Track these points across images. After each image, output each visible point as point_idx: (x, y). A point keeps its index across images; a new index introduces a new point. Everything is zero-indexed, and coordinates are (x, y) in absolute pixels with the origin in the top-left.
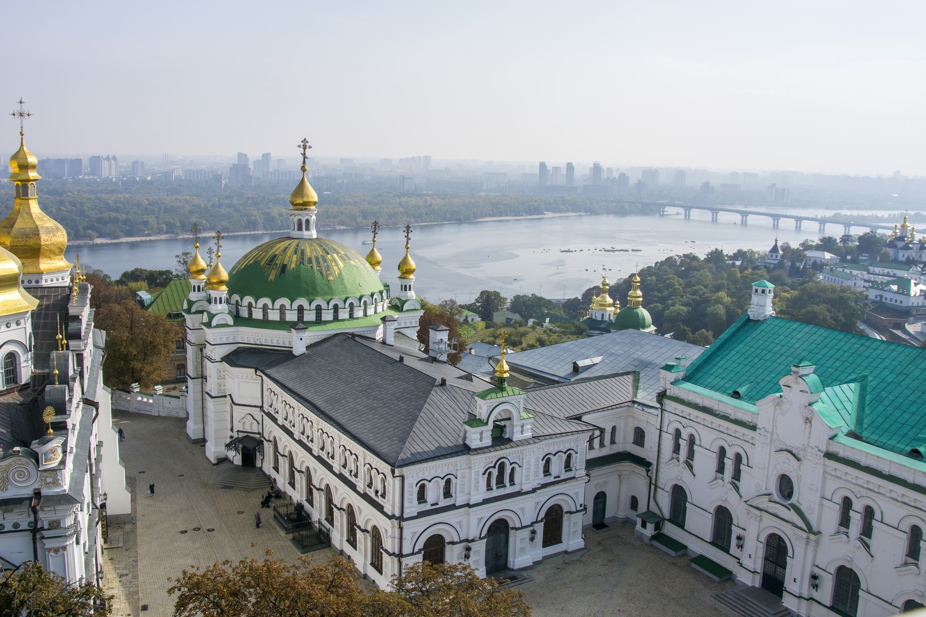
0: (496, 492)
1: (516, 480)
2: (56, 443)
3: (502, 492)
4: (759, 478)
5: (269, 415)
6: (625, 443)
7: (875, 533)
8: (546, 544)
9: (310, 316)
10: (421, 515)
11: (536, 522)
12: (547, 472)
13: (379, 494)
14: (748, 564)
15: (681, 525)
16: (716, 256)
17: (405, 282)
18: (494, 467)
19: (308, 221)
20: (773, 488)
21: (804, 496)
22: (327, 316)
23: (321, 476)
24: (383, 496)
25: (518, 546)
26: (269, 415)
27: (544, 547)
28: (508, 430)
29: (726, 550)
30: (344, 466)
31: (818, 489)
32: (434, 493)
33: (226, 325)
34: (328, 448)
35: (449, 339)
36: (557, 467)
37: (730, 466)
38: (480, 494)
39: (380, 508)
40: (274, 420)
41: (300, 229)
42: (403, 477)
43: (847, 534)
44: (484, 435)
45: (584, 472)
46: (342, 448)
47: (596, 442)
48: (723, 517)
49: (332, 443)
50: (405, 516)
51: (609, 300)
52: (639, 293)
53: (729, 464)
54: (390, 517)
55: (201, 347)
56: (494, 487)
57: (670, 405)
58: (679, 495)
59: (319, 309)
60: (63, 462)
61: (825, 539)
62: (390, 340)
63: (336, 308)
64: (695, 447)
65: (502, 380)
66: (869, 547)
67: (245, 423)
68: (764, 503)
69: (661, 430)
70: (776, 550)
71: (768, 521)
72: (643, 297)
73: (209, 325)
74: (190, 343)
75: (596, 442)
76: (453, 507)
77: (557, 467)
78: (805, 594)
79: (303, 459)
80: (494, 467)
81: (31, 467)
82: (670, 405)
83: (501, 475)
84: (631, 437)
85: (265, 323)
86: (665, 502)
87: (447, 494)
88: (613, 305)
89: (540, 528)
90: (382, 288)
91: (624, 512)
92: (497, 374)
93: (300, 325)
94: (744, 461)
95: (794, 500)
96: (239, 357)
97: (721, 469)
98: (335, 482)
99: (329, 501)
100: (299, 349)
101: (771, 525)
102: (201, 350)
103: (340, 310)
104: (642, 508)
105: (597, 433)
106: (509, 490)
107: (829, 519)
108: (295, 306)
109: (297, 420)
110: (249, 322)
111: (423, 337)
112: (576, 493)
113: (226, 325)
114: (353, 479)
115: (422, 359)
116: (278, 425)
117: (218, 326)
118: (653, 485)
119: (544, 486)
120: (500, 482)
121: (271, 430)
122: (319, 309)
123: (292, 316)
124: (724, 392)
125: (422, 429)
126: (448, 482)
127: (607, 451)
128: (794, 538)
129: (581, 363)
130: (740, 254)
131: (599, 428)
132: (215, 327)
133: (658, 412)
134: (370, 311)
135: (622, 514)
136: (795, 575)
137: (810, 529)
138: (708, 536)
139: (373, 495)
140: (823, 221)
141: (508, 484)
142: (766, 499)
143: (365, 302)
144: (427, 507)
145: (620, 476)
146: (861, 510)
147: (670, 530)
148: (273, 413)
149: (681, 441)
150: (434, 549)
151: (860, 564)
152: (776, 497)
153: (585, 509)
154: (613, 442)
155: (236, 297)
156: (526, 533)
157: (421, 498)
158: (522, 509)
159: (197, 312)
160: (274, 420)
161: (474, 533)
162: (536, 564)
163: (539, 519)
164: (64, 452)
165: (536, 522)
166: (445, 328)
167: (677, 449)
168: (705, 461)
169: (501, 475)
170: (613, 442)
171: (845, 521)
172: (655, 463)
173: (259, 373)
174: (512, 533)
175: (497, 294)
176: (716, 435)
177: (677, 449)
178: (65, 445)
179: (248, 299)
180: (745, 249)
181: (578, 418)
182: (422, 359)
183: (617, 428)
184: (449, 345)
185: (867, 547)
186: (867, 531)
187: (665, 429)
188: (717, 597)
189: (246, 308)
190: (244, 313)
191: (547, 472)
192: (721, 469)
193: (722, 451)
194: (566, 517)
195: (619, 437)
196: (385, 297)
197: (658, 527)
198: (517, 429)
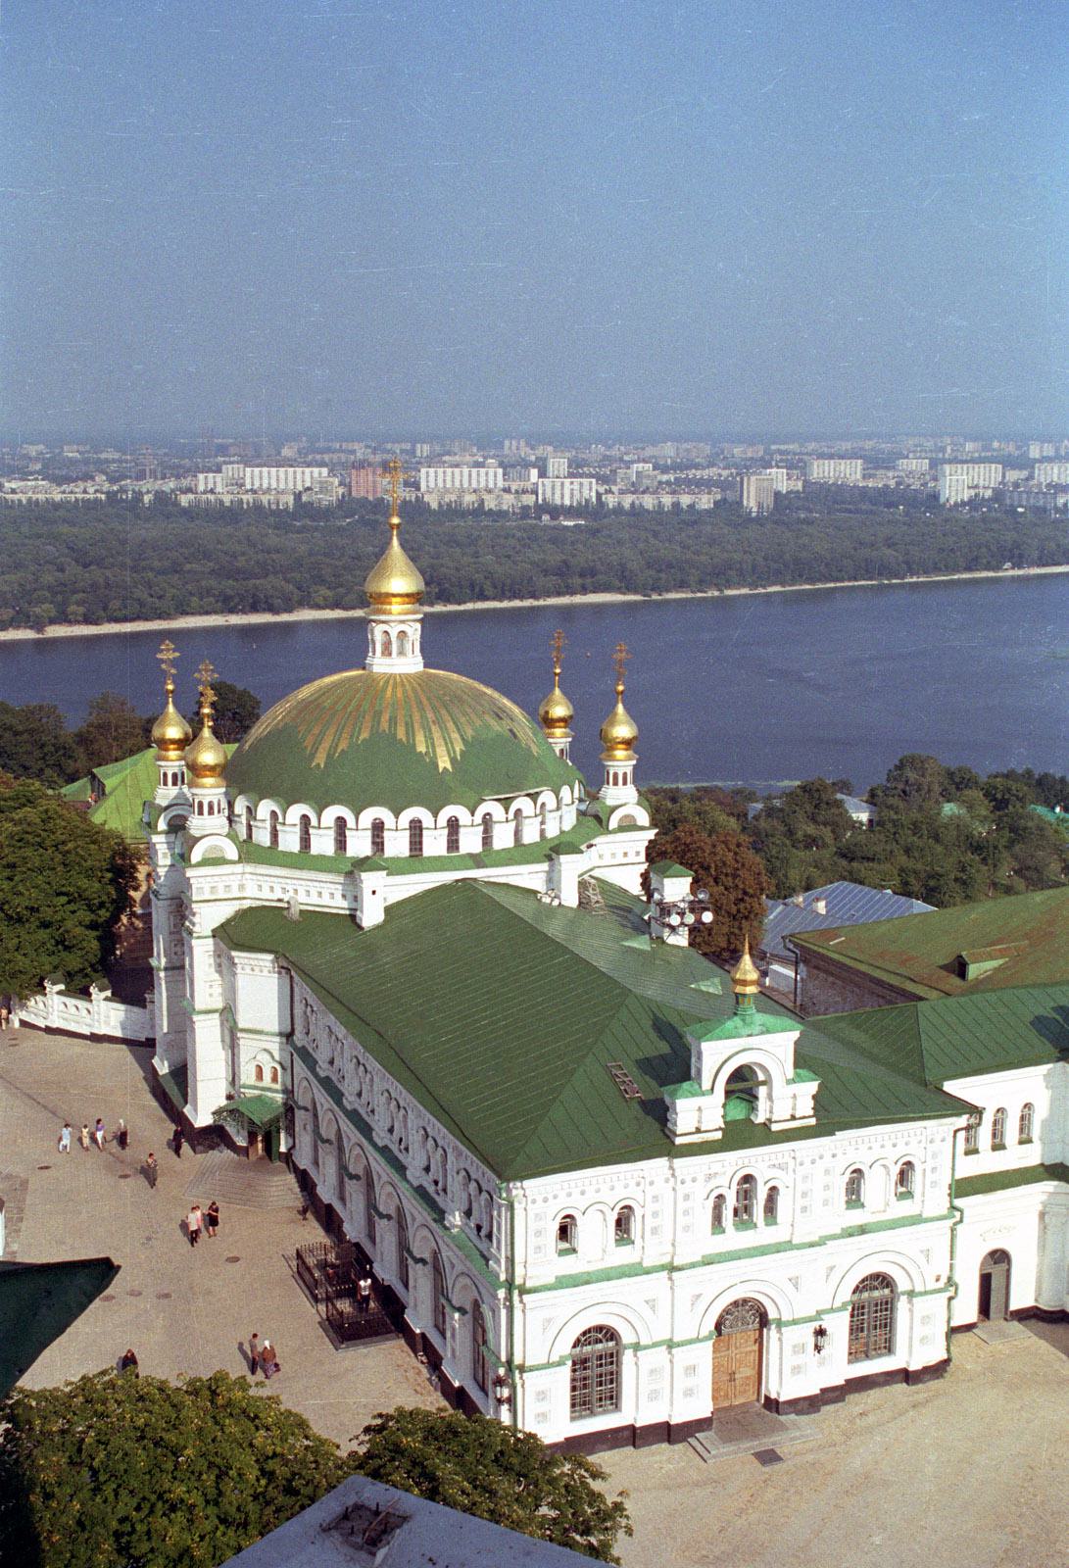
8: (854, 1356)
9: (397, 845)
11: (832, 1310)
13: (483, 1233)
19: (402, 634)
22: (435, 844)
25: (790, 1360)
27: (850, 1362)
41: (387, 651)
45: (943, 1207)
77: (878, 1188)
83: (748, 1202)
85: (304, 859)
89: (839, 1326)
103: (462, 831)
110: (270, 855)
113: (220, 861)
117: (205, 862)
119: (849, 1233)
132: (199, 865)
143: (518, 812)
158: (795, 1282)
163: (838, 1304)
179: (265, 808)
189: (268, 824)
190: (262, 837)
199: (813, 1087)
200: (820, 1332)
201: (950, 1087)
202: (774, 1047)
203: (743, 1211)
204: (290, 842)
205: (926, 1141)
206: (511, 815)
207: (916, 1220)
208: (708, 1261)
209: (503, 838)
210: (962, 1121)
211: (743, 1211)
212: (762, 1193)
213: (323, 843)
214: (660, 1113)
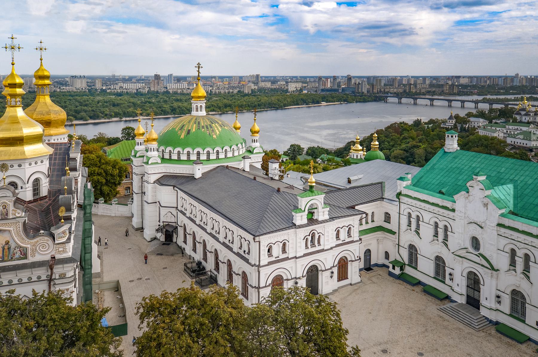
1: (322, 243)
2: (66, 227)
3: (314, 249)
4: (460, 239)
5: (181, 212)
6: (379, 221)
7: (532, 270)
9: (203, 157)
10: (270, 263)
12: (338, 237)
14: (458, 289)
16: (417, 123)
17: (254, 138)
18: (309, 235)
20: (468, 244)
22: (213, 157)
23: (212, 244)
24: (249, 253)
26: (181, 212)
28: (316, 214)
30: (226, 238)
31: (494, 246)
32: (277, 251)
33: (157, 163)
34: (216, 228)
35: (280, 167)
36: (343, 235)
37: (442, 233)
39: (247, 261)
40: (184, 214)
42: (259, 242)
43: (515, 270)
44: (303, 217)
46: (224, 227)
47: (364, 221)
49: (219, 225)
50: (261, 265)
51: (360, 148)
52: (377, 143)
53: (441, 232)
54: (253, 266)
55: (143, 176)
56: (309, 247)
57: (404, 199)
59: (208, 154)
60: (69, 239)
61: (502, 274)
62: (247, 169)
63: (218, 152)
64: (420, 223)
65: (311, 187)
66: (529, 278)
67: (167, 218)
68: (463, 253)
69: (399, 214)
71: (467, 264)
72: (379, 145)
73: (147, 163)
74: (135, 174)
75: (364, 221)
76: (287, 259)
77: (343, 235)
79: (201, 235)
80: (309, 235)
81: (50, 242)
82: (404, 199)
83: (313, 240)
85: (179, 161)
87: (284, 251)
88: (363, 150)
90: (242, 141)
92: (309, 184)
93: (198, 162)
94: (450, 229)
95: (481, 251)
96: (165, 180)
97: (436, 235)
98: (219, 247)
99: (217, 258)
100: (198, 175)
102: (142, 178)
105: (364, 215)
106: (318, 248)
108: (195, 152)
109: (198, 214)
111: (265, 167)
112: (355, 251)
113: (157, 163)
114: (231, 245)
115: (265, 178)
116: (187, 217)
120: (313, 245)
121: (182, 220)
122: (208, 154)
123: (194, 157)
124: (434, 192)
125: (269, 215)
126: (284, 245)
127: (371, 225)
128: (483, 274)
129: (352, 178)
130: (431, 121)
131: (365, 213)
133: (397, 203)
134: (236, 154)
136: (487, 295)
137: (493, 268)
139: (242, 253)
141: (317, 245)
142: (465, 251)
144: (273, 259)
145: (378, 240)
146: (523, 256)
148: (183, 210)
149: (412, 219)
150: (278, 281)
151: (524, 287)
152: (471, 250)
154: (373, 221)
155: (162, 148)
159: (140, 157)
160: (184, 214)
164: (70, 233)
165: (334, 266)
166: (277, 161)
167: (409, 225)
168: (427, 231)
169: (313, 240)
170: (373, 221)
171: (513, 263)
172: (397, 232)
173: (175, 188)
174: (320, 273)
176: (431, 215)
177: (409, 225)
178: (70, 229)
180: (434, 119)
181: (353, 207)
182: (265, 178)
183: (375, 214)
184: (280, 171)
185: (528, 277)
186: (527, 268)
187: (401, 212)
190: (167, 156)
191: (338, 237)
192: (436, 235)
193: (436, 225)
194: (349, 263)
196: (244, 146)
198: (321, 214)
199: (328, 209)
200: (332, 273)
201: (356, 207)
202: (319, 199)
203: (312, 241)
204: (175, 157)
205: (354, 221)
206: (224, 151)
207: (352, 242)
208: (305, 255)
209: (230, 155)
210: (364, 215)
211: (312, 241)
212: (317, 236)
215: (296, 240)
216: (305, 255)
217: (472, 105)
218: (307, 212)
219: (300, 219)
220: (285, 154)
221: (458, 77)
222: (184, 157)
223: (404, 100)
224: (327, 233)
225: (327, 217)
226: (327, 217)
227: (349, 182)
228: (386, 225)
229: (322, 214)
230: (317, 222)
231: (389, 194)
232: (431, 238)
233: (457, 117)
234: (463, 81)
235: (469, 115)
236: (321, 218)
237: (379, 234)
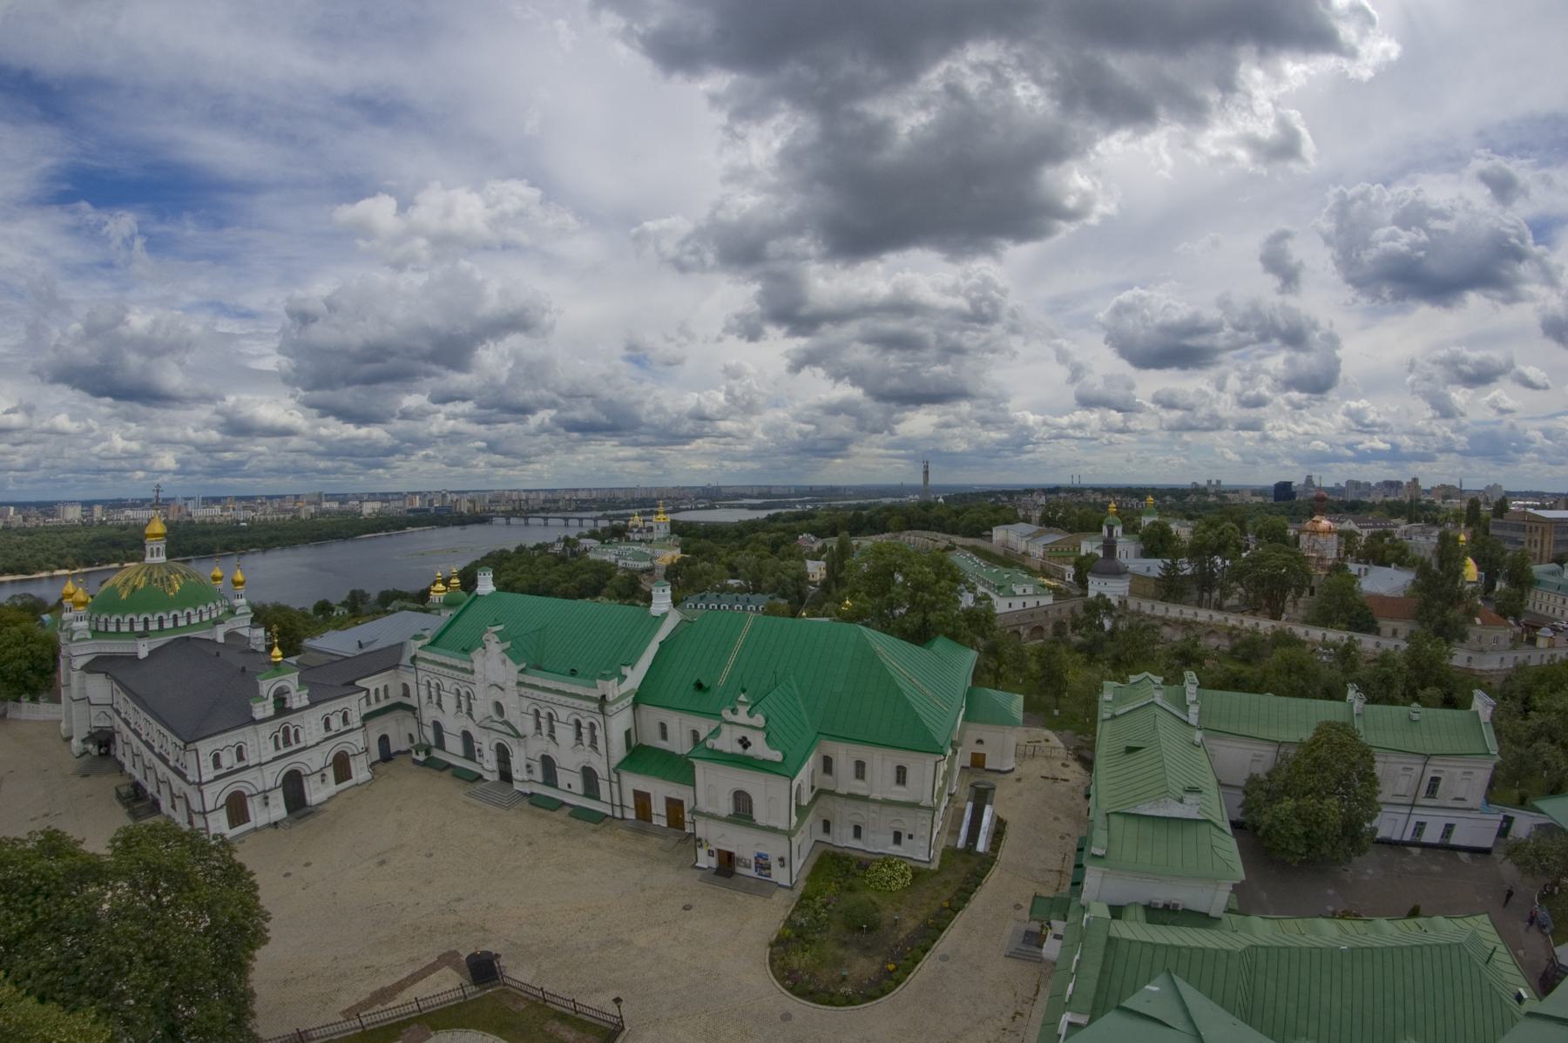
0: (284, 751)
3: (290, 749)
6: (396, 696)
8: (338, 782)
12: (327, 726)
15: (443, 749)
20: (492, 712)
21: (512, 714)
29: (473, 760)
32: (228, 760)
36: (336, 724)
38: (270, 753)
48: (467, 737)
58: (437, 727)
70: (503, 754)
71: (494, 735)
76: (247, 767)
77: (336, 724)
78: (526, 777)
84: (400, 690)
86: (430, 734)
89: (330, 773)
91: (405, 746)
100: (143, 653)
101: (495, 738)
104: (417, 741)
106: (295, 747)
107: (527, 726)
118: (420, 723)
119: (327, 739)
120: (287, 743)
126: (240, 749)
127: (384, 703)
128: (511, 744)
135: (403, 748)
137: (518, 735)
138: (461, 753)
140: (596, 520)
144: (223, 771)
147: (437, 753)
152: (496, 718)
153: (367, 750)
154: (387, 697)
156: (318, 777)
157: (217, 764)
161: (270, 784)
162: (330, 799)
171: (538, 726)
175: (362, 592)
186: (552, 730)
188: (469, 794)
191: (327, 726)
195: (391, 693)
197: (428, 752)
202: (291, 681)
204: (112, 628)
212: (292, 731)
213: (125, 628)
214: (250, 710)
215: (259, 743)
216: (275, 759)
217: (592, 523)
218: (271, 699)
219: (263, 709)
220: (344, 604)
221: (576, 490)
222: (125, 628)
223: (513, 520)
224: (310, 726)
225: (307, 702)
226: (307, 702)
227: (361, 646)
228: (406, 700)
229: (298, 699)
230: (291, 711)
231: (406, 660)
232: (454, 709)
233: (567, 540)
234: (583, 495)
235: (581, 536)
236: (295, 706)
237: (399, 714)
